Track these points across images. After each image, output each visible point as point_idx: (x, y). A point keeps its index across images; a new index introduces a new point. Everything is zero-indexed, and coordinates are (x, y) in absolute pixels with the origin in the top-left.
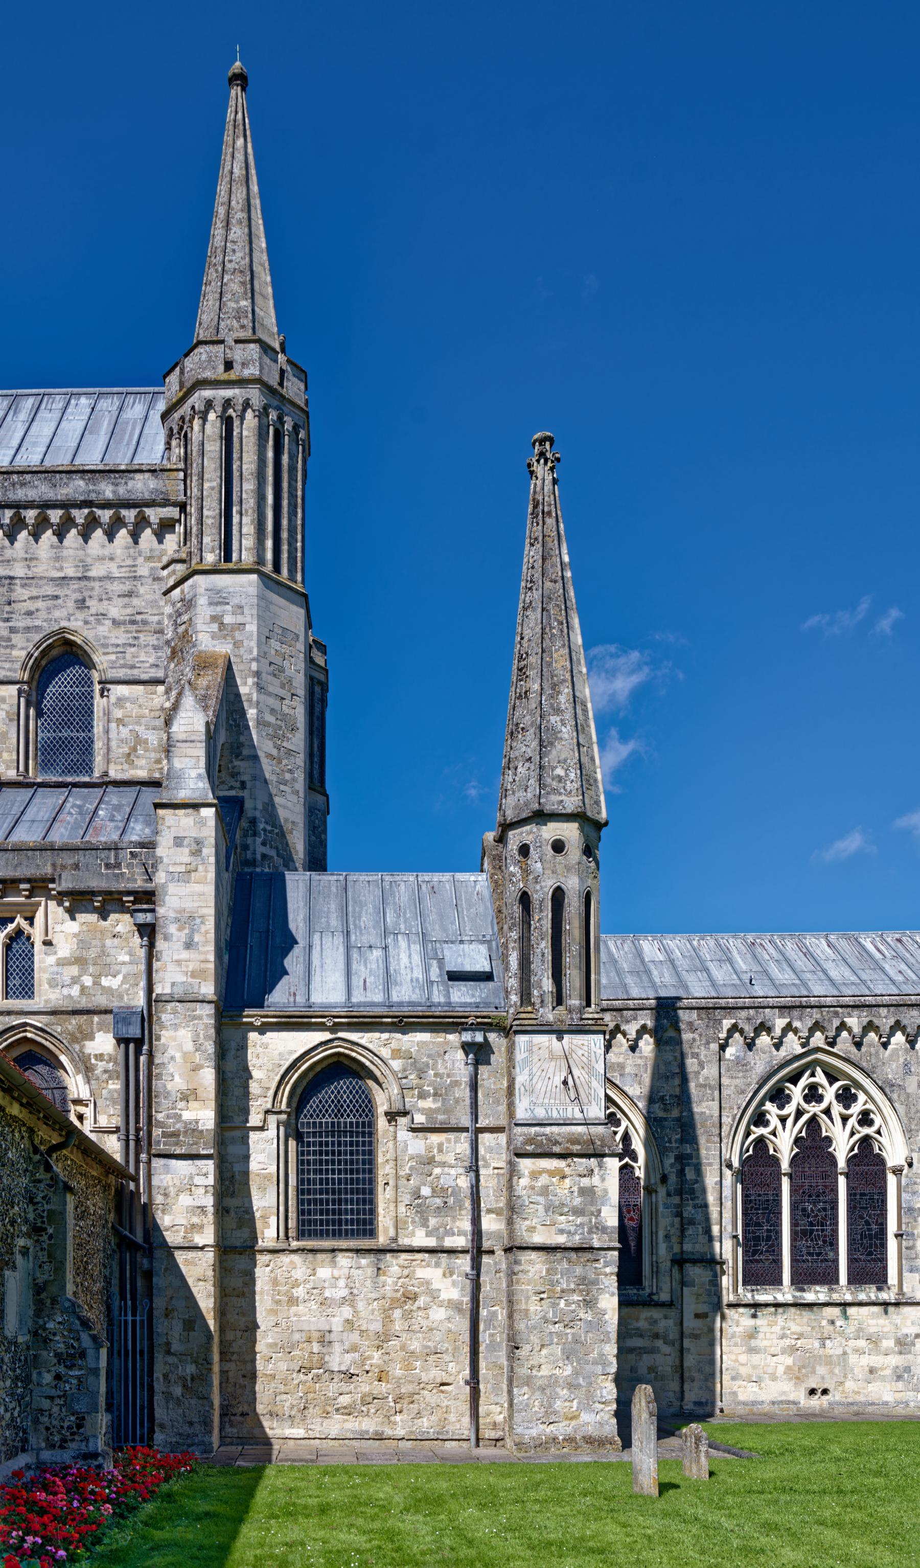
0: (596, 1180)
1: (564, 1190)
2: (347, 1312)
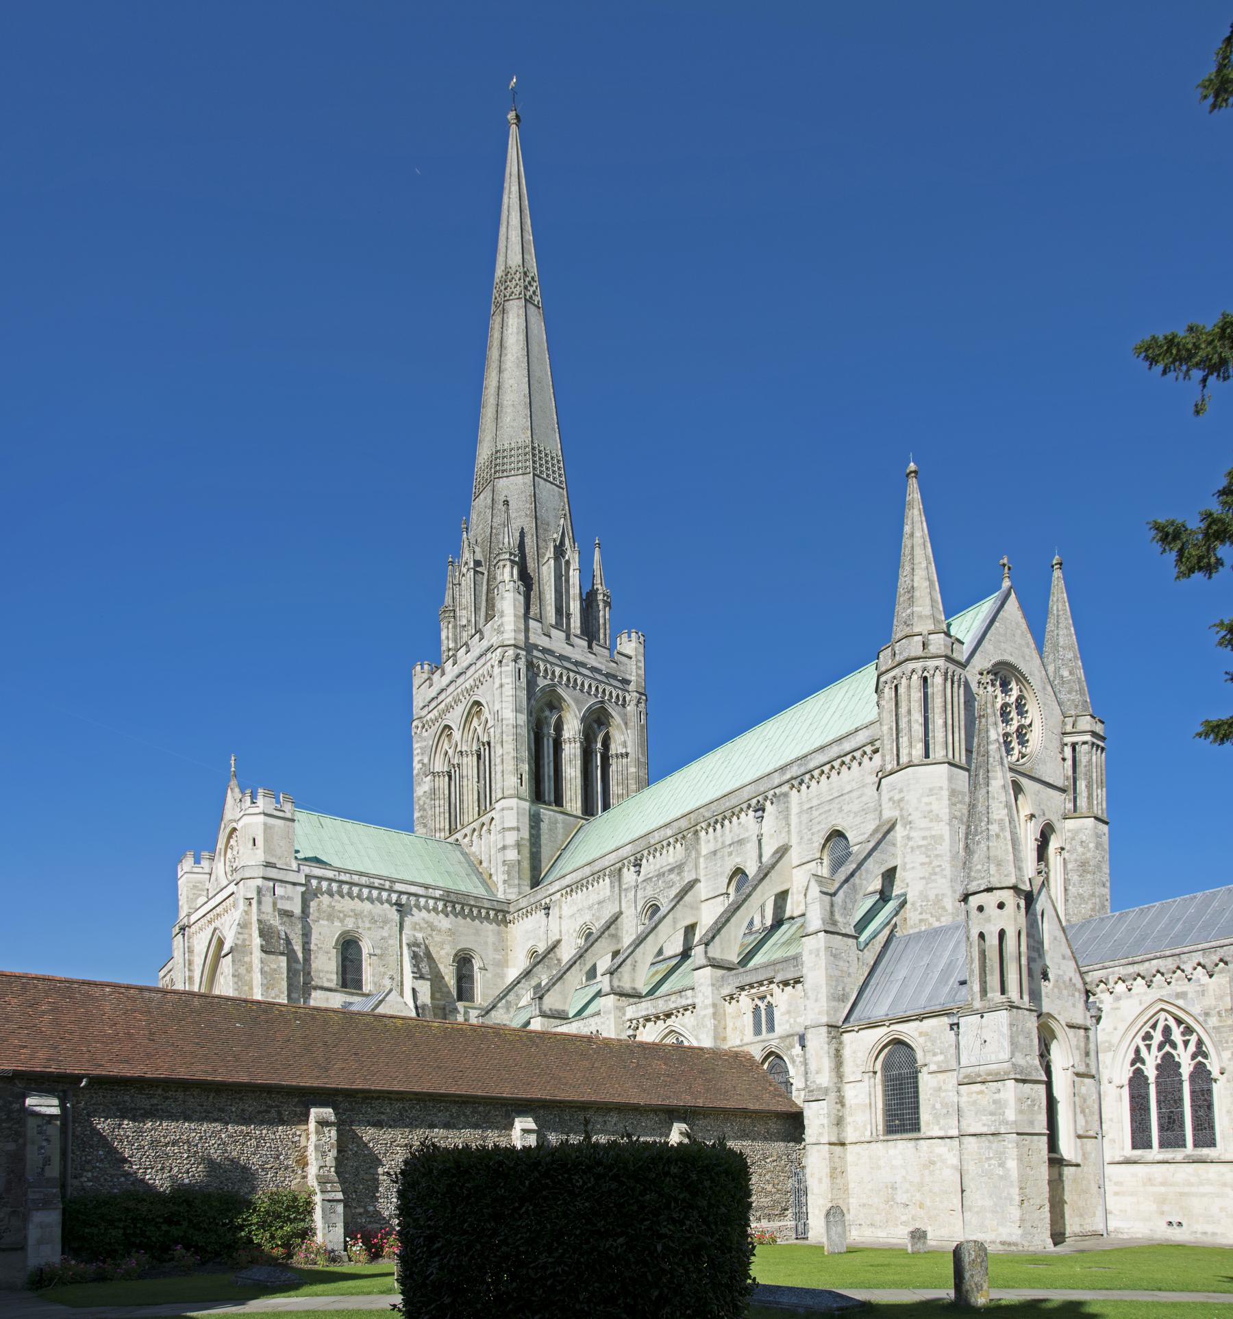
0: (1002, 1095)
1: (984, 1101)
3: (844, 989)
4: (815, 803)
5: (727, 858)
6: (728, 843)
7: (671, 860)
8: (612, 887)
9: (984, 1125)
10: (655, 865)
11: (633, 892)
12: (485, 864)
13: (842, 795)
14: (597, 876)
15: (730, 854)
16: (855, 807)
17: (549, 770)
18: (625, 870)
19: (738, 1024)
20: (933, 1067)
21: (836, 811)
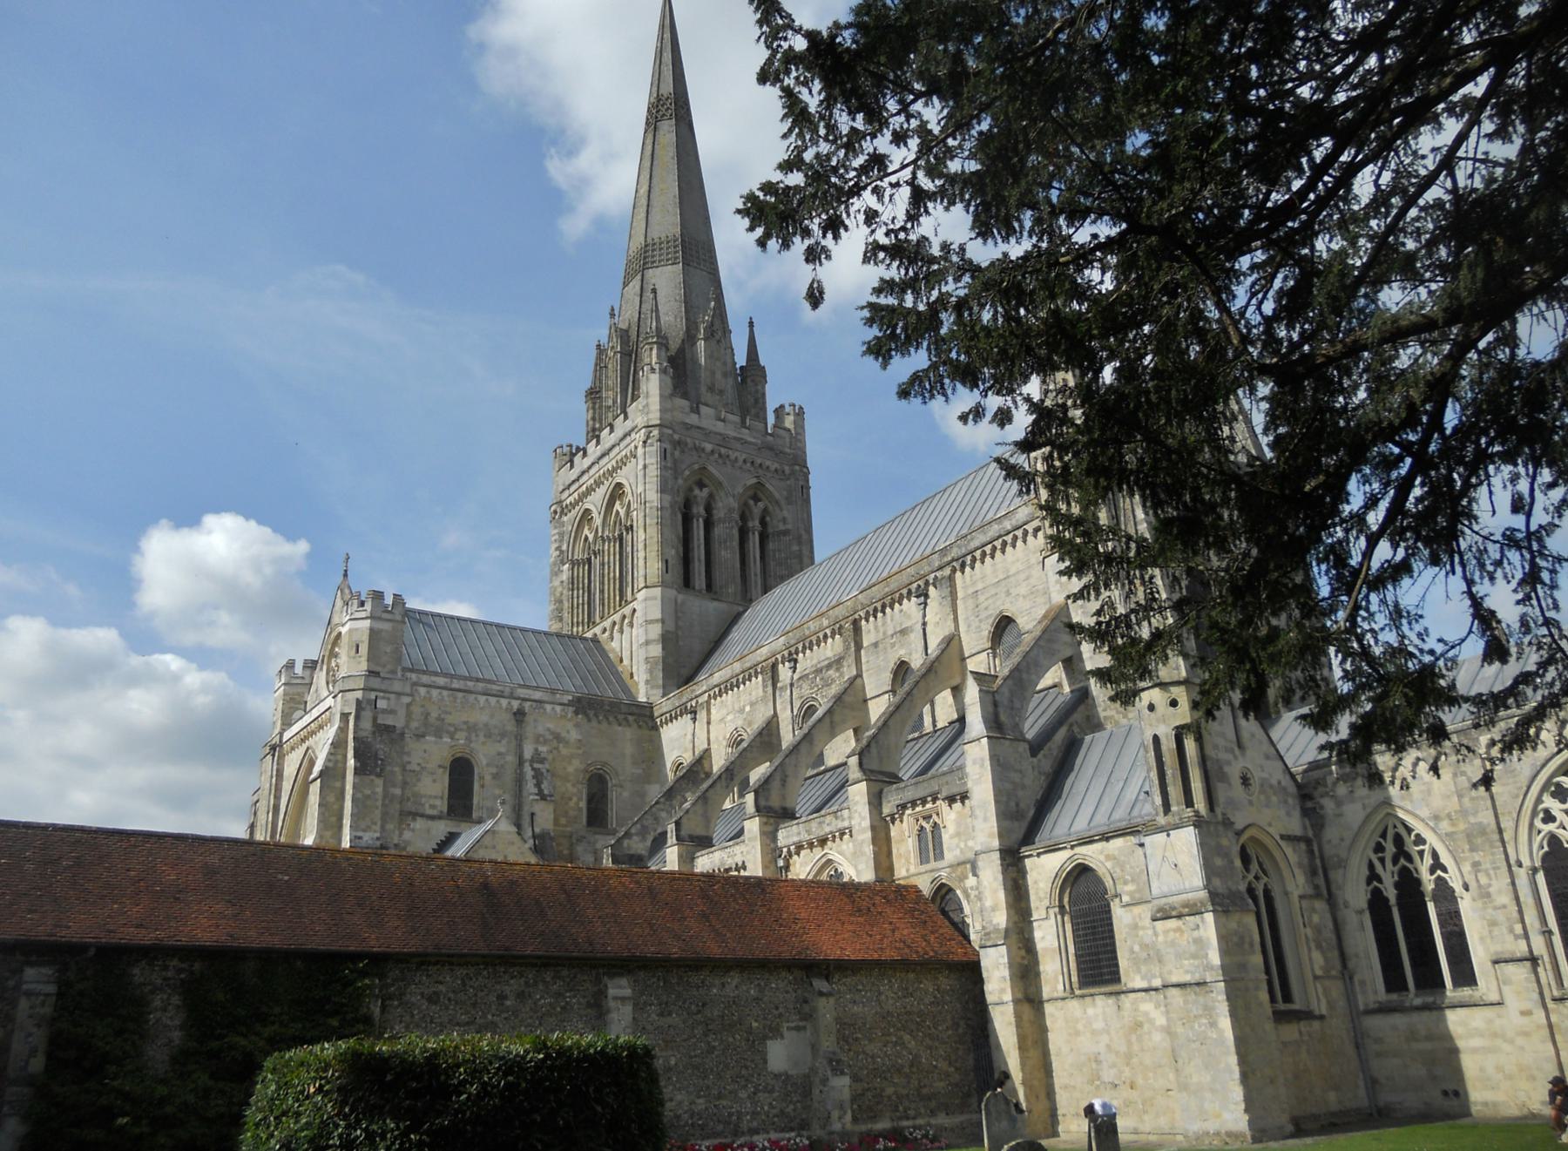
0: (1202, 932)
1: (1184, 941)
2: (1105, 1039)
3: (1017, 805)
4: (980, 586)
5: (889, 650)
6: (890, 632)
7: (829, 654)
8: (765, 686)
9: (1187, 972)
10: (812, 659)
11: (788, 691)
12: (626, 662)
13: (1008, 577)
14: (748, 675)
15: (893, 645)
16: (1023, 590)
17: (699, 552)
18: (781, 666)
19: (902, 851)
20: (1126, 899)
21: (1003, 595)
